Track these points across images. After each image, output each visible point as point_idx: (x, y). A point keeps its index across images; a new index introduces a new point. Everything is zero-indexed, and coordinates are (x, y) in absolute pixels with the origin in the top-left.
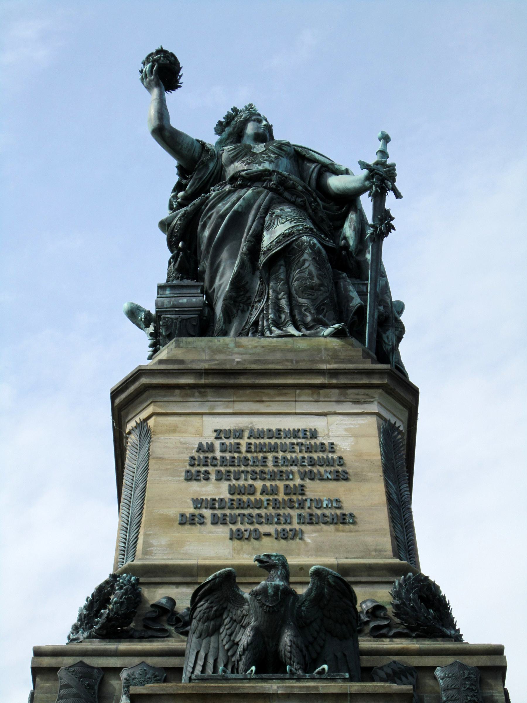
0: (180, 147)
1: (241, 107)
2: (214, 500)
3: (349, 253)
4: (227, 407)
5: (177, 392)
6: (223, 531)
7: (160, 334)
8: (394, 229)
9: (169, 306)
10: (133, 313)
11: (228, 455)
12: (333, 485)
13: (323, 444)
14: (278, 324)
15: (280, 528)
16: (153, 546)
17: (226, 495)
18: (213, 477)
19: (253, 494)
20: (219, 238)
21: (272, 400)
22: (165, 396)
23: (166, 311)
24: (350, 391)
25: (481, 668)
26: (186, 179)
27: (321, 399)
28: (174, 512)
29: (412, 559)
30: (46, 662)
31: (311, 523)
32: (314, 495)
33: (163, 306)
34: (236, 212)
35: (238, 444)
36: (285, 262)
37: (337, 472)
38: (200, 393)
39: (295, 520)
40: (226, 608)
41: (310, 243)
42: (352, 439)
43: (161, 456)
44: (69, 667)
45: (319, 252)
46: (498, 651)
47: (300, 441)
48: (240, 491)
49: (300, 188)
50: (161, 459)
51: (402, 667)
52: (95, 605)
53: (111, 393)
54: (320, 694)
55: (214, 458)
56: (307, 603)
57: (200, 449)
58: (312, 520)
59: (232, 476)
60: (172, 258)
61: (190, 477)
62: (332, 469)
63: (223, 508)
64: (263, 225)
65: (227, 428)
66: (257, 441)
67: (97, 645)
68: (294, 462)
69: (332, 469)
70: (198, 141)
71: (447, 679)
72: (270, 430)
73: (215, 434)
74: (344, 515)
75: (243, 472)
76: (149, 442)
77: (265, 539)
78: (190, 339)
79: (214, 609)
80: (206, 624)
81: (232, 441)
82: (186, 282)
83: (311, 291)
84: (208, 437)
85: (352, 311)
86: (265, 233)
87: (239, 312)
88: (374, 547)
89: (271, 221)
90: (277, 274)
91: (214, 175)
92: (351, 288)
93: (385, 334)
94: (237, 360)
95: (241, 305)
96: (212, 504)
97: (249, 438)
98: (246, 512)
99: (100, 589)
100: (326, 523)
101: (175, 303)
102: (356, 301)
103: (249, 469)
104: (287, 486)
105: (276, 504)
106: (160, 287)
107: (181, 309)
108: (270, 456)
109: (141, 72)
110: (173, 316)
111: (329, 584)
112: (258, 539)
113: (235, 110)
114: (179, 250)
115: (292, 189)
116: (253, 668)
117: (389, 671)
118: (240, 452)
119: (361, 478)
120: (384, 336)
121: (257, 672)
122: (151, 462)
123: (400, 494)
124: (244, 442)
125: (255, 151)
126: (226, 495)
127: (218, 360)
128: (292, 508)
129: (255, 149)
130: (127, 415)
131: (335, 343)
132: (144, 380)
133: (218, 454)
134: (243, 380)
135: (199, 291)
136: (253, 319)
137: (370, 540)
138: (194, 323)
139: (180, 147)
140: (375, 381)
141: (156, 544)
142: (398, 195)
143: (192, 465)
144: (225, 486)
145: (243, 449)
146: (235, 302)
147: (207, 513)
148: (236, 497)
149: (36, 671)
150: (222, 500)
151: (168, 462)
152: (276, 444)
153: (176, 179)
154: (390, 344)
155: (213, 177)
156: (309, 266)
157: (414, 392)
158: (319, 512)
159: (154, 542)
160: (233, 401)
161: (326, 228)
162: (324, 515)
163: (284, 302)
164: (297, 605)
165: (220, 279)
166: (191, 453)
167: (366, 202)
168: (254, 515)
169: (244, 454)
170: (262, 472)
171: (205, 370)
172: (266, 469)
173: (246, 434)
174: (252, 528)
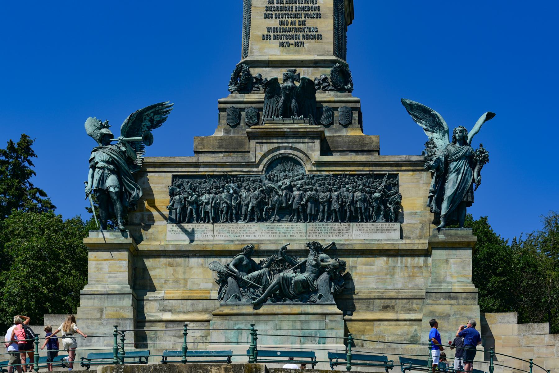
2: (274, 28)
6: (277, 43)
11: (279, 5)
12: (315, 20)
17: (279, 26)
18: (274, 16)
19: (287, 25)
25: (352, 108)
30: (222, 106)
39: (301, 37)
50: (255, 7)
55: (274, 7)
61: (266, 17)
62: (315, 12)
63: (277, 32)
68: (302, 9)
69: (315, 12)
77: (291, 46)
96: (273, 30)
100: (312, 39)
103: (287, 12)
104: (299, 21)
105: (295, 30)
108: (294, 5)
112: (289, 46)
118: (283, 4)
119: (326, 18)
126: (279, 26)
128: (301, 32)
133: (276, 5)
137: (326, 46)
143: (267, 11)
144: (278, 20)
148: (282, 26)
150: (277, 28)
162: (311, 35)
169: (285, 5)
170: (291, 14)
172: (292, 12)
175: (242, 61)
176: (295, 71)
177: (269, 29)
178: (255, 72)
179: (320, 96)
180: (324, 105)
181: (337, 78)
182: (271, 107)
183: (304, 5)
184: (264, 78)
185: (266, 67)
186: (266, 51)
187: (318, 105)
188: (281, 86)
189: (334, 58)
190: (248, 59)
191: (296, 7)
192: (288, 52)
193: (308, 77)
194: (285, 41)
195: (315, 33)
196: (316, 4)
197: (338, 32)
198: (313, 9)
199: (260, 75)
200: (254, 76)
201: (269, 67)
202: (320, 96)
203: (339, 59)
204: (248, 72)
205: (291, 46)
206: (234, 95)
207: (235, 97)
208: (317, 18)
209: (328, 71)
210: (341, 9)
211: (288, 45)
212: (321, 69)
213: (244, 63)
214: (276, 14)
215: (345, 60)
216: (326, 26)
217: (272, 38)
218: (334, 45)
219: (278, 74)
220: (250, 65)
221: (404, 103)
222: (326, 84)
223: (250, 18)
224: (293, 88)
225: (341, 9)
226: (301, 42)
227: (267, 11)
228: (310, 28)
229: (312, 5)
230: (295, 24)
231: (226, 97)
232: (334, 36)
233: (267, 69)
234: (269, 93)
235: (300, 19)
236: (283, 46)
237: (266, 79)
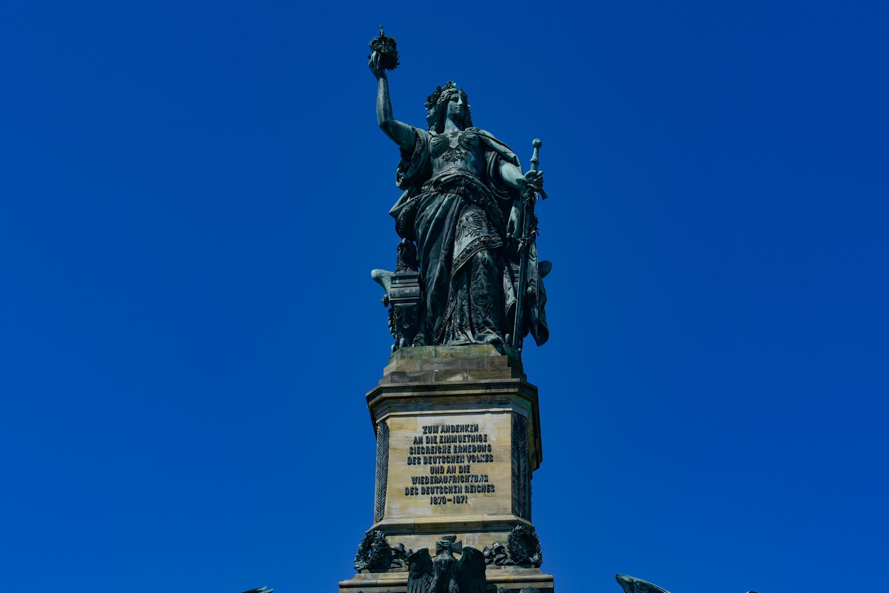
6: (427, 499)
11: (430, 445)
14: (461, 328)
15: (456, 495)
17: (429, 475)
18: (422, 461)
19: (443, 473)
31: (472, 492)
39: (464, 490)
42: (496, 431)
47: (470, 433)
49: (480, 189)
50: (395, 449)
55: (423, 448)
58: (472, 490)
61: (411, 462)
62: (484, 453)
63: (427, 483)
66: (446, 434)
68: (465, 449)
77: (448, 503)
84: (419, 433)
98: (439, 485)
100: (479, 492)
103: (441, 455)
104: (460, 467)
108: (452, 445)
112: (444, 503)
119: (500, 460)
122: (390, 451)
124: (438, 435)
128: (462, 482)
132: (384, 395)
133: (425, 445)
137: (501, 502)
140: (511, 390)
142: (544, 196)
143: (412, 454)
144: (429, 466)
145: (438, 440)
147: (419, 486)
148: (434, 475)
156: (482, 279)
158: (476, 484)
162: (479, 487)
163: (466, 308)
169: (439, 444)
175: (375, 526)
176: (455, 538)
178: (394, 542)
179: (491, 574)
180: (499, 586)
181: (517, 546)
183: (467, 444)
184: (407, 549)
185: (410, 534)
187: (489, 587)
188: (433, 560)
189: (512, 517)
190: (383, 522)
193: (474, 547)
194: (439, 495)
195: (483, 483)
196: (486, 441)
197: (519, 481)
198: (481, 449)
199: (402, 546)
200: (392, 547)
201: (415, 534)
202: (491, 574)
203: (520, 519)
204: (384, 541)
205: (448, 503)
206: (362, 575)
207: (365, 578)
209: (504, 537)
210: (523, 447)
211: (444, 501)
212: (493, 534)
213: (378, 528)
214: (425, 458)
215: (530, 521)
216: (501, 472)
217: (420, 491)
218: (513, 499)
219: (430, 543)
220: (387, 532)
221: (620, 581)
222: (501, 556)
223: (387, 465)
224: (452, 563)
225: (523, 447)
226: (463, 497)
227: (412, 454)
228: (476, 477)
229: (479, 443)
230: (454, 471)
231: (350, 578)
232: (513, 487)
233: (413, 537)
234: (415, 570)
236: (436, 504)
237: (411, 550)
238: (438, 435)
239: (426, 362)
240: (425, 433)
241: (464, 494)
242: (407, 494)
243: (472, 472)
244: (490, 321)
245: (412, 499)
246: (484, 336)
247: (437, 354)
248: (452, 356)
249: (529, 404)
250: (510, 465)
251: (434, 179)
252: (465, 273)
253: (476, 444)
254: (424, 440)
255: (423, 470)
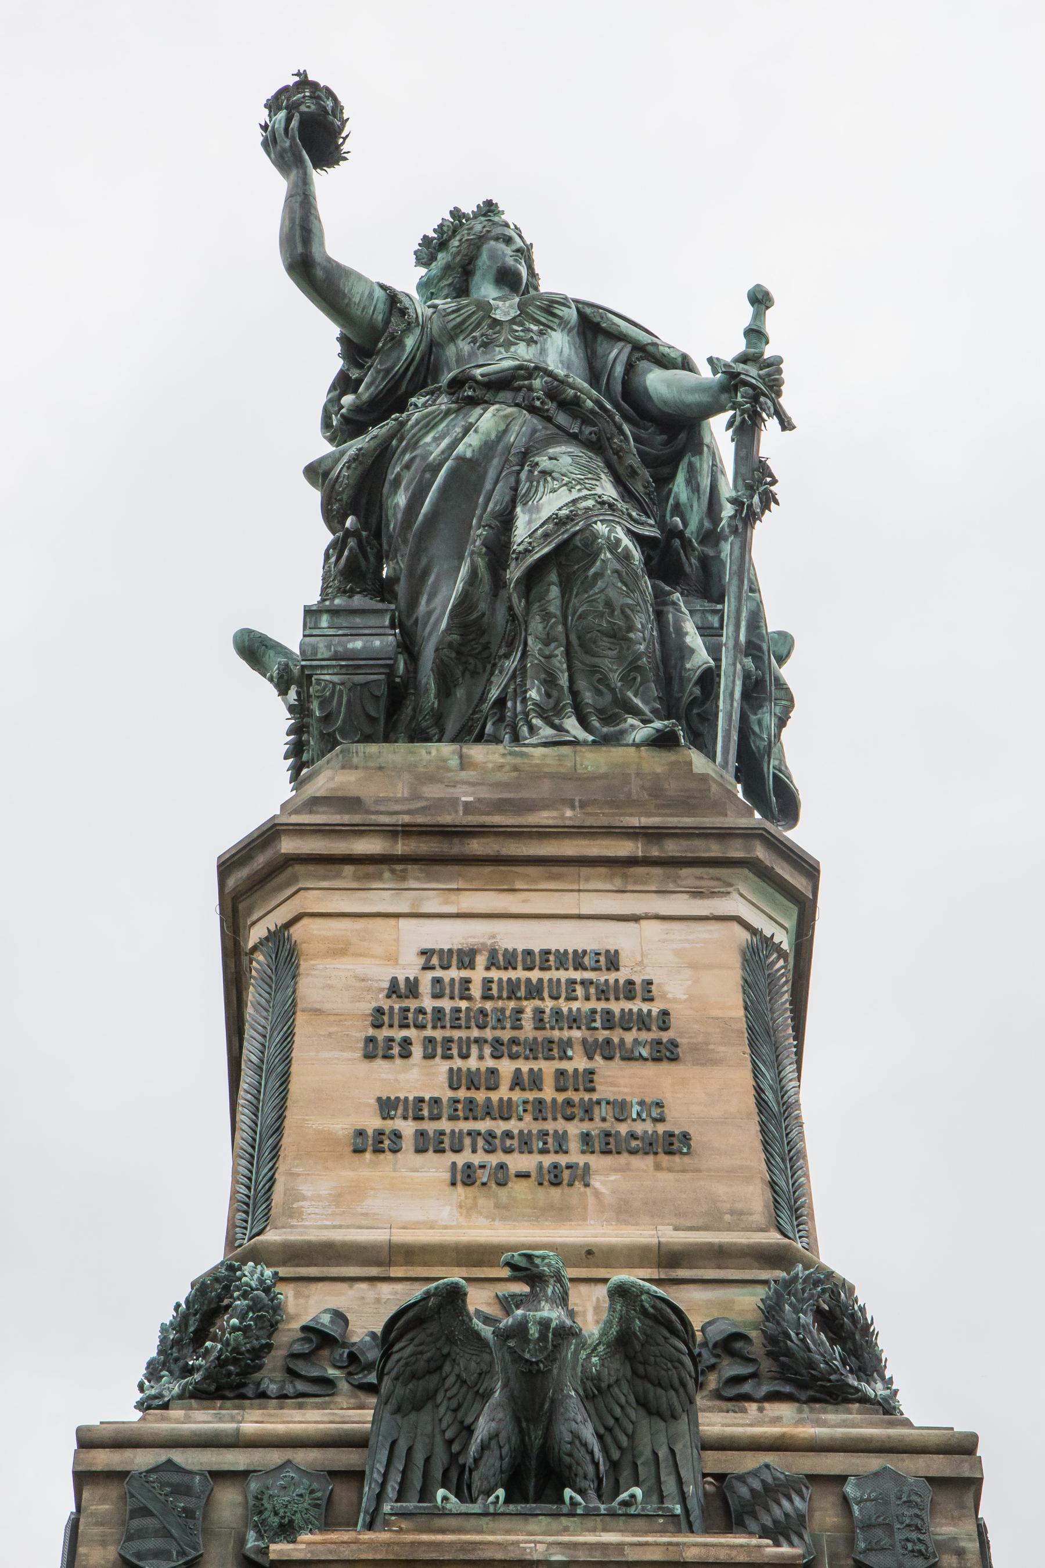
0: (346, 301)
1: (468, 208)
2: (421, 1100)
3: (686, 543)
4: (446, 902)
5: (349, 869)
6: (435, 1168)
7: (310, 714)
8: (777, 503)
9: (327, 655)
10: (253, 649)
11: (446, 1004)
12: (650, 1071)
13: (630, 983)
15: (547, 1160)
16: (304, 1198)
18: (417, 1051)
19: (494, 1088)
20: (426, 515)
21: (533, 887)
22: (324, 878)
23: (322, 667)
24: (685, 872)
26: (360, 366)
27: (630, 888)
28: (342, 1126)
29: (801, 1227)
30: (103, 1459)
31: (606, 1152)
32: (614, 1093)
33: (316, 654)
34: (461, 459)
35: (468, 981)
36: (560, 575)
37: (659, 1043)
38: (393, 872)
39: (574, 1145)
40: (448, 1354)
41: (609, 538)
42: (689, 972)
43: (317, 1006)
44: (149, 1471)
45: (627, 556)
46: (965, 1447)
47: (588, 975)
48: (472, 1081)
49: (589, 404)
50: (317, 1012)
51: (782, 1477)
52: (191, 1322)
53: (219, 867)
54: (627, 1562)
55: (421, 1011)
56: (601, 1348)
57: (393, 989)
58: (608, 1145)
59: (455, 1052)
60: (333, 545)
61: (372, 1050)
64: (515, 489)
65: (446, 947)
67: (203, 1420)
68: (574, 1021)
70: (383, 287)
71: (868, 1503)
72: (529, 953)
73: (421, 961)
74: (672, 1135)
75: (477, 1041)
76: (294, 977)
78: (373, 748)
79: (426, 1356)
80: (410, 1386)
81: (454, 973)
82: (359, 601)
83: (611, 640)
84: (409, 967)
85: (690, 680)
86: (518, 509)
87: (467, 675)
88: (728, 1206)
89: (531, 483)
90: (544, 602)
91: (415, 363)
92: (689, 626)
93: (756, 714)
94: (463, 799)
95: (471, 660)
96: (416, 1109)
97: (488, 969)
98: (484, 1126)
99: (201, 1288)
100: (633, 1152)
101: (340, 649)
102: (701, 657)
103: (488, 1034)
105: (539, 1110)
106: (309, 612)
107: (351, 663)
108: (529, 1006)
109: (265, 127)
110: (336, 679)
111: (644, 1312)
113: (456, 213)
114: (348, 534)
115: (571, 406)
116: (501, 1492)
117: (757, 1485)
118: (469, 998)
119: (705, 1057)
120: (753, 718)
121: (508, 1500)
122: (300, 1018)
123: (780, 1090)
124: (478, 975)
125: (498, 317)
127: (427, 799)
128: (569, 1118)
129: (498, 312)
130: (250, 911)
131: (657, 762)
133: (428, 1003)
134: (476, 847)
135: (387, 623)
136: (494, 693)
137: (721, 1190)
138: (378, 694)
139: (346, 301)
141: (309, 1194)
142: (786, 424)
143: (378, 1026)
144: (442, 1067)
145: (476, 991)
146: (459, 653)
147: (408, 1128)
148: (462, 1094)
149: (82, 1478)
150: (436, 1101)
151: (332, 1018)
152: (541, 980)
153: (337, 364)
154: (765, 736)
155: (412, 368)
157: (810, 870)
158: (623, 1129)
159: (306, 1189)
160: (458, 889)
161: (641, 489)
162: (633, 1136)
164: (583, 1355)
165: (429, 602)
166: (377, 1000)
167: (719, 431)
168: (499, 1132)
170: (514, 1041)
171: (403, 825)
172: (521, 1035)
173: (481, 960)
174: (494, 1160)
177: (387, 1107)
182: (419, 1459)
186: (376, 1204)
191: (539, 1012)
192: (505, 1211)
206: (173, 1413)
207: (187, 1420)
208: (657, 1060)
211: (501, 1176)
216: (710, 1097)
223: (287, 1059)
235: (565, 1065)
238: (478, 975)
239: (431, 778)
240: (426, 968)
241: (575, 1156)
242: (358, 1151)
243: (603, 1091)
244: (637, 701)
245: (371, 1169)
246: (623, 732)
247: (464, 763)
248: (515, 768)
249: (794, 911)
250: (745, 1077)
251: (446, 377)
252: (554, 577)
253: (616, 1007)
254: (425, 987)
255: (421, 1078)
